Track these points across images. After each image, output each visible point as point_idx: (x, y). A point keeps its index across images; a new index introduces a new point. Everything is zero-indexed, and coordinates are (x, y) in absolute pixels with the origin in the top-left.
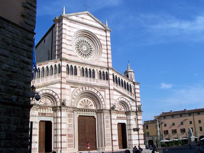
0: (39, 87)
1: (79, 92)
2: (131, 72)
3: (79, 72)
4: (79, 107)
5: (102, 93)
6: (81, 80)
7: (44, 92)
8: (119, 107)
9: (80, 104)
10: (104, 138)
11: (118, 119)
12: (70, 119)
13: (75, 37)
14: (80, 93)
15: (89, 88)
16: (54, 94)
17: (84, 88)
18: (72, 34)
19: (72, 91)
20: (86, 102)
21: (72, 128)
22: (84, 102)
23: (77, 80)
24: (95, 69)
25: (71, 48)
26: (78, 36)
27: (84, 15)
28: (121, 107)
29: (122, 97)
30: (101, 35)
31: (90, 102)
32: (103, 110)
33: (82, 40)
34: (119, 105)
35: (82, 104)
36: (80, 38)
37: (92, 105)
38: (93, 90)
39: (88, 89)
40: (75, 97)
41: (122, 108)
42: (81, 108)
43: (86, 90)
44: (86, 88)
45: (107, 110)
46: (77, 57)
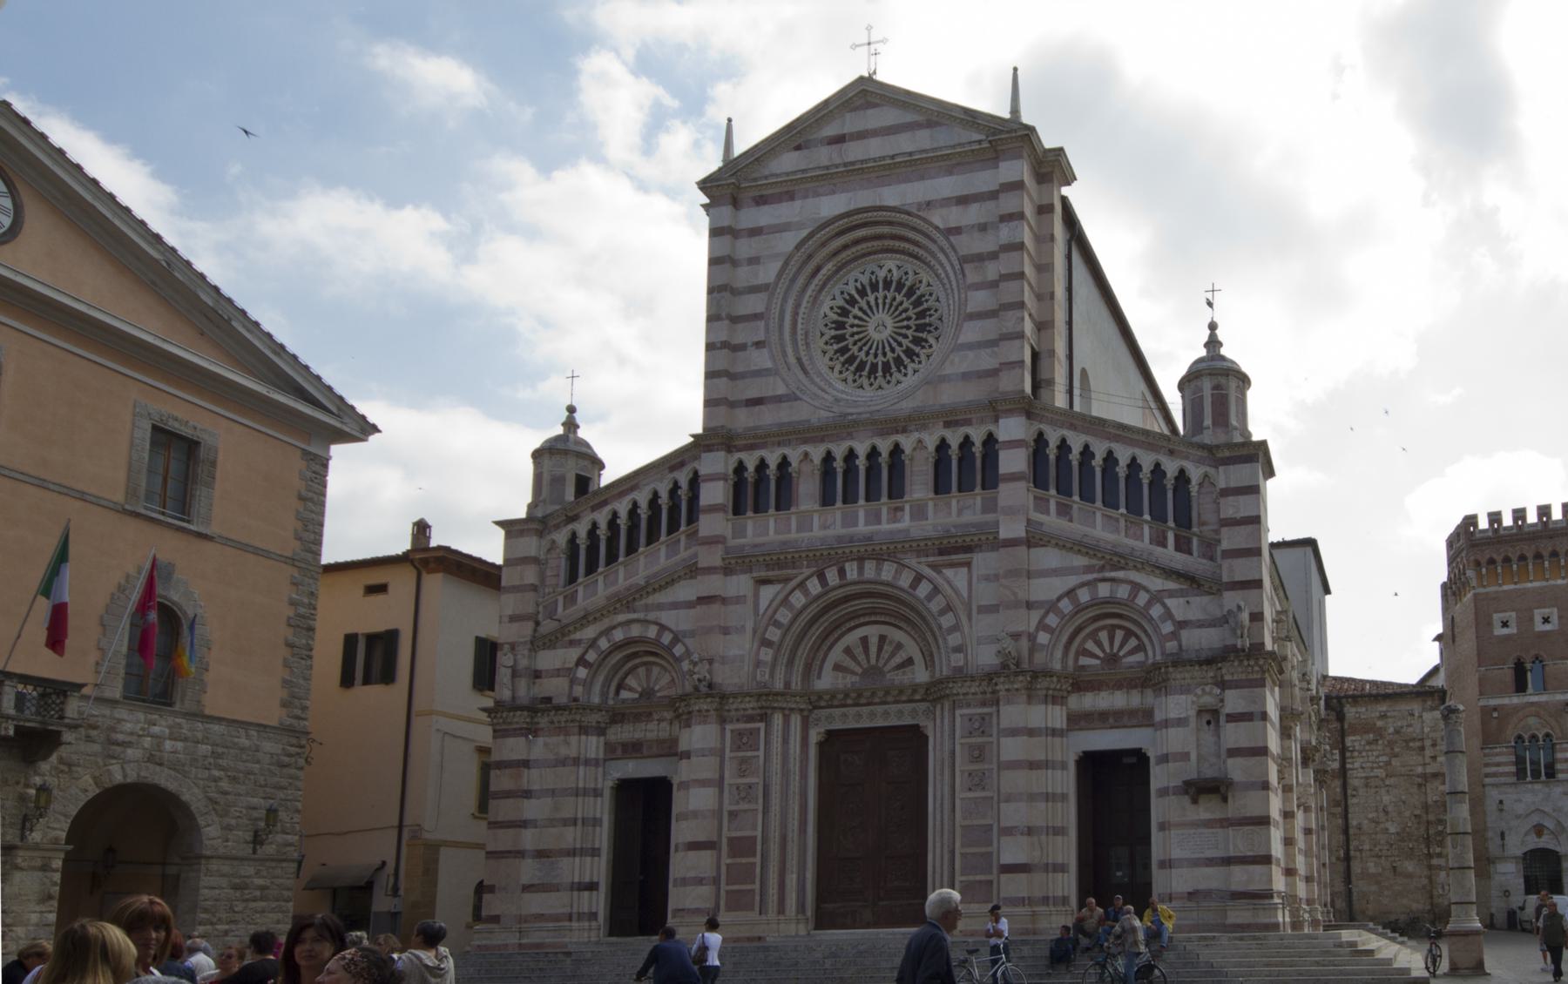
0: (591, 618)
1: (798, 599)
2: (1223, 380)
3: (807, 488)
4: (826, 681)
5: (958, 577)
6: (817, 532)
7: (619, 635)
8: (1099, 644)
9: (837, 667)
10: (953, 852)
12: (743, 761)
13: (801, 281)
14: (805, 607)
15: (861, 569)
16: (666, 639)
17: (832, 577)
18: (767, 273)
19: (763, 604)
20: (873, 649)
21: (752, 806)
22: (858, 651)
23: (793, 535)
24: (907, 442)
25: (761, 359)
26: (830, 266)
28: (1121, 646)
29: (1100, 575)
30: (963, 201)
31: (899, 646)
34: (1103, 636)
37: (909, 662)
38: (888, 572)
39: (855, 572)
40: (774, 634)
41: (1121, 654)
44: (842, 572)
46: (797, 399)
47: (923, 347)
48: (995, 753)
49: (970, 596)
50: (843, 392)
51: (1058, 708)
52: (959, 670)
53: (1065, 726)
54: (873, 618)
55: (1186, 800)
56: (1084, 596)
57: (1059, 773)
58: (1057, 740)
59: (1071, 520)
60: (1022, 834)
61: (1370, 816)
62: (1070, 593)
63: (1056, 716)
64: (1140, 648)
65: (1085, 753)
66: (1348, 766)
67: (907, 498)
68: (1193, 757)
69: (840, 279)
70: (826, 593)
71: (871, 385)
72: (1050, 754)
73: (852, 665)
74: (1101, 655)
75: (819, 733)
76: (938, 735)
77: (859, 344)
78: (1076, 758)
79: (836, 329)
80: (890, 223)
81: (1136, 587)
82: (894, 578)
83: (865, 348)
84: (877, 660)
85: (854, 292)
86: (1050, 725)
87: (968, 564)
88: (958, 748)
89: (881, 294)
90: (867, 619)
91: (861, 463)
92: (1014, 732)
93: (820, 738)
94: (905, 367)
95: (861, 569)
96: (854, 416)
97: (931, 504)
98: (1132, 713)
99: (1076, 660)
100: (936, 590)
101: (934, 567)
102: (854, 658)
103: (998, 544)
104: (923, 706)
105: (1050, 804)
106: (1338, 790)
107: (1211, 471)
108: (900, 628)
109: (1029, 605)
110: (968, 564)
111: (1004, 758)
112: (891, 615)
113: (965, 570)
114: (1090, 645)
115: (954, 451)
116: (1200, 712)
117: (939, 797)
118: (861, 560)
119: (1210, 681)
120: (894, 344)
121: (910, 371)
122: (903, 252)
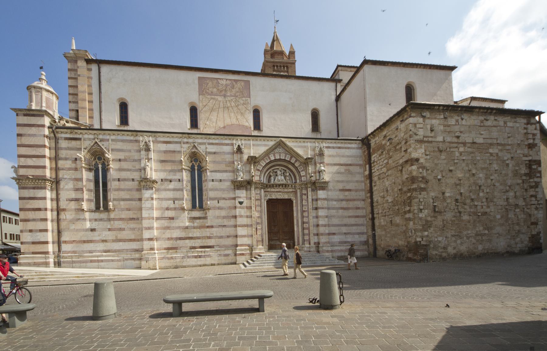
61: (381, 195)
66: (373, 171)
106: (368, 185)
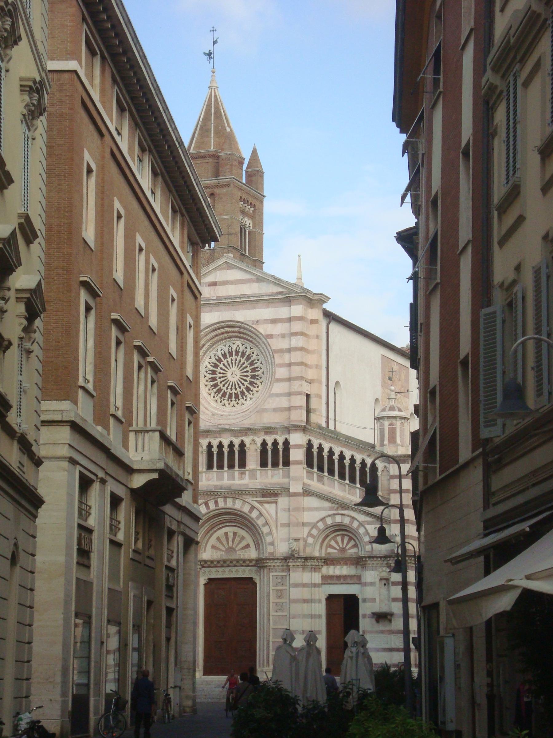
5: (270, 508)
9: (213, 547)
10: (268, 641)
11: (330, 582)
15: (225, 502)
17: (212, 506)
20: (230, 539)
22: (223, 539)
24: (247, 440)
27: (218, 272)
31: (243, 538)
32: (263, 559)
33: (227, 351)
35: (218, 545)
36: (220, 346)
37: (248, 546)
38: (238, 505)
39: (223, 503)
41: (347, 548)
42: (215, 558)
43: (218, 508)
44: (216, 503)
45: (278, 559)
47: (255, 387)
48: (288, 594)
49: (277, 518)
50: (216, 408)
51: (317, 573)
52: (272, 553)
53: (320, 582)
54: (233, 524)
55: (373, 620)
56: (329, 521)
57: (317, 605)
58: (317, 589)
59: (323, 484)
60: (300, 634)
62: (323, 519)
63: (317, 578)
64: (355, 546)
65: (329, 595)
67: (247, 468)
68: (377, 600)
69: (213, 349)
70: (209, 513)
71: (229, 404)
72: (313, 595)
73: (221, 547)
74: (338, 548)
75: (205, 580)
76: (262, 584)
77: (223, 383)
78: (326, 597)
79: (212, 374)
80: (239, 327)
81: (353, 518)
82: (241, 507)
83: (226, 385)
84: (232, 545)
85: (220, 356)
86: (313, 582)
87: (276, 502)
88: (271, 591)
89: (234, 358)
90: (228, 524)
91: (226, 450)
92: (297, 585)
93: (205, 582)
94: (246, 397)
95: (225, 502)
96: (222, 426)
97: (258, 472)
98: (352, 577)
99: (326, 550)
100: (261, 514)
101: (259, 502)
102: (222, 543)
103: (289, 494)
104: (254, 568)
105: (313, 620)
107: (387, 465)
108: (244, 529)
109: (304, 524)
110: (276, 502)
111: (292, 597)
112: (239, 523)
113: (274, 505)
114: (333, 543)
115: (269, 447)
116: (381, 579)
117: (262, 612)
118: (225, 498)
119: (385, 565)
120: (240, 384)
121: (248, 399)
122: (245, 339)
